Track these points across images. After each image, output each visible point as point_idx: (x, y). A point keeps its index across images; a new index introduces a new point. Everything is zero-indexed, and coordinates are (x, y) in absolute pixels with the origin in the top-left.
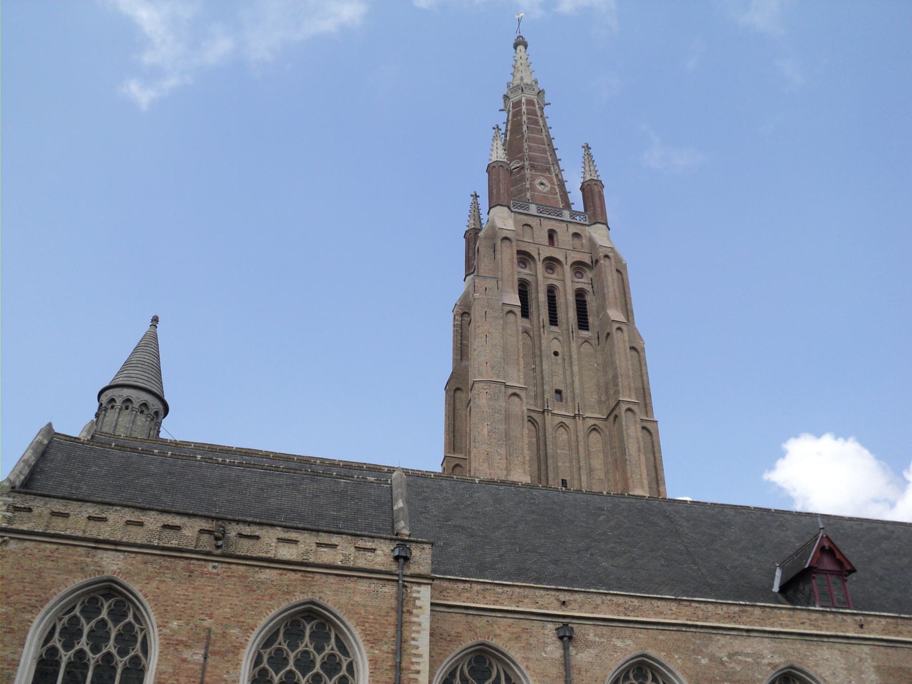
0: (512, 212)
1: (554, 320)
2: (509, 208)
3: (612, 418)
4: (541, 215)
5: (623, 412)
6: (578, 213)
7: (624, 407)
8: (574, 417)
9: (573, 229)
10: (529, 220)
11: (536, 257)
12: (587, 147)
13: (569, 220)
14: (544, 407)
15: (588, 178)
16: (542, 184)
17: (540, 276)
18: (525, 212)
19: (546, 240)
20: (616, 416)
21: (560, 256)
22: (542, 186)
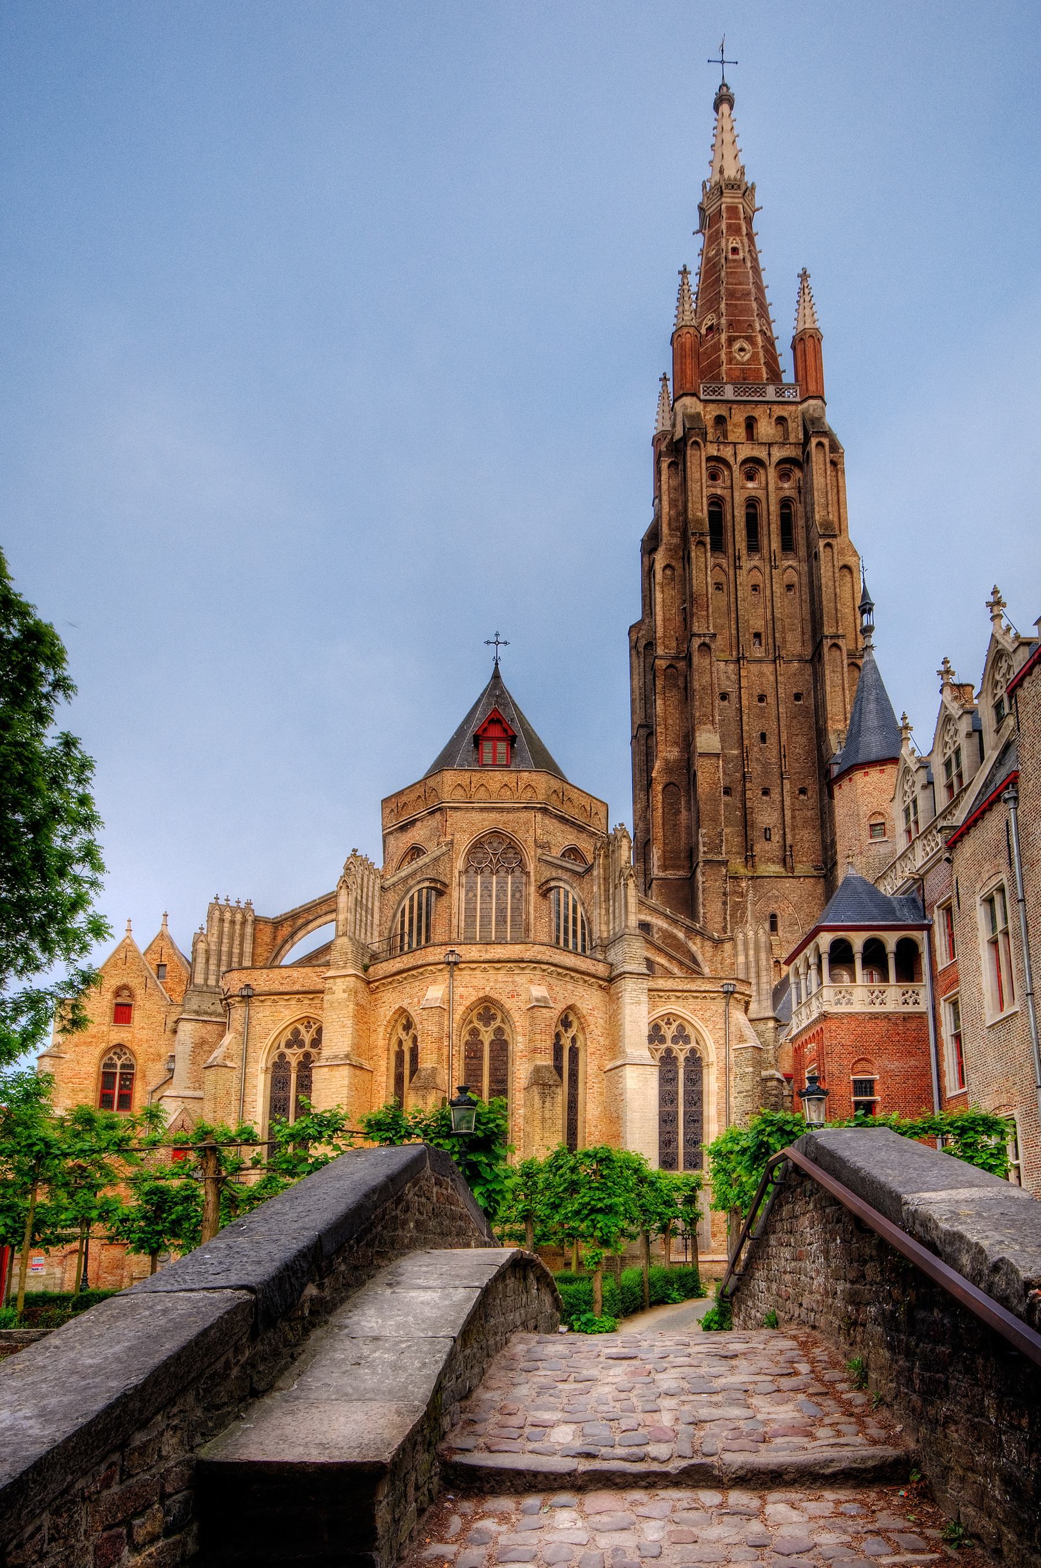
0: (701, 400)
4: (739, 398)
6: (789, 386)
18: (719, 398)
22: (742, 354)
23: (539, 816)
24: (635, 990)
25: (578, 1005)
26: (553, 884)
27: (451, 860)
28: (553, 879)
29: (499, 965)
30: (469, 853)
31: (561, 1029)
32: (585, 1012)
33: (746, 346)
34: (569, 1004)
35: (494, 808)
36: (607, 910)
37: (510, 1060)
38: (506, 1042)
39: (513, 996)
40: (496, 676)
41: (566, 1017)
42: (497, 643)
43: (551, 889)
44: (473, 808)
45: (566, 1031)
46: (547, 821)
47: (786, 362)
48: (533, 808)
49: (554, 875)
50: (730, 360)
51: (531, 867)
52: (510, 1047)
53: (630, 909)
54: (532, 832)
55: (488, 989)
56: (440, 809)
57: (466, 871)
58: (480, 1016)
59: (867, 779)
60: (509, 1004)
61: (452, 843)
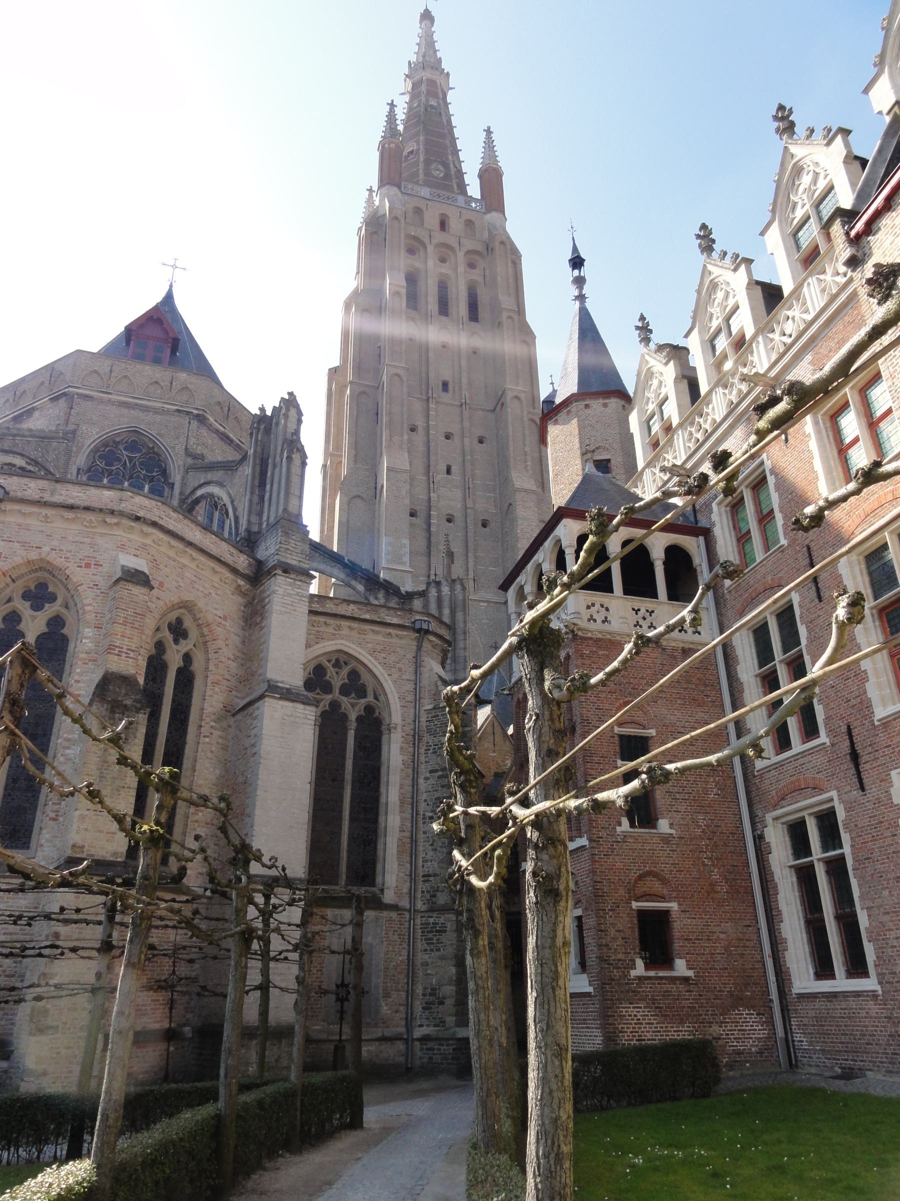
0: (402, 193)
1: (444, 308)
2: (400, 190)
3: (499, 406)
5: (508, 398)
6: (476, 200)
7: (509, 395)
8: (461, 405)
9: (468, 215)
10: (422, 204)
11: (426, 240)
12: (488, 132)
13: (463, 205)
14: (428, 393)
15: (488, 162)
16: (438, 170)
17: (430, 263)
19: (437, 226)
20: (503, 404)
21: (453, 242)
23: (195, 424)
24: (290, 595)
25: (201, 604)
26: (199, 493)
27: (68, 453)
28: (201, 486)
29: (70, 515)
30: (95, 451)
31: (168, 636)
32: (210, 618)
33: (441, 168)
34: (187, 597)
35: (136, 404)
36: (262, 498)
37: (67, 667)
38: (65, 640)
39: (88, 566)
40: (169, 298)
41: (179, 621)
42: (174, 267)
43: (197, 501)
44: (109, 400)
45: (176, 641)
46: (204, 431)
47: (474, 189)
48: (188, 413)
49: (202, 481)
50: (427, 173)
51: (177, 477)
52: (71, 646)
53: (292, 491)
54: (183, 439)
55: (46, 549)
56: (65, 394)
57: (89, 470)
58: (26, 596)
59: (588, 411)
60: (77, 575)
61: (74, 432)
